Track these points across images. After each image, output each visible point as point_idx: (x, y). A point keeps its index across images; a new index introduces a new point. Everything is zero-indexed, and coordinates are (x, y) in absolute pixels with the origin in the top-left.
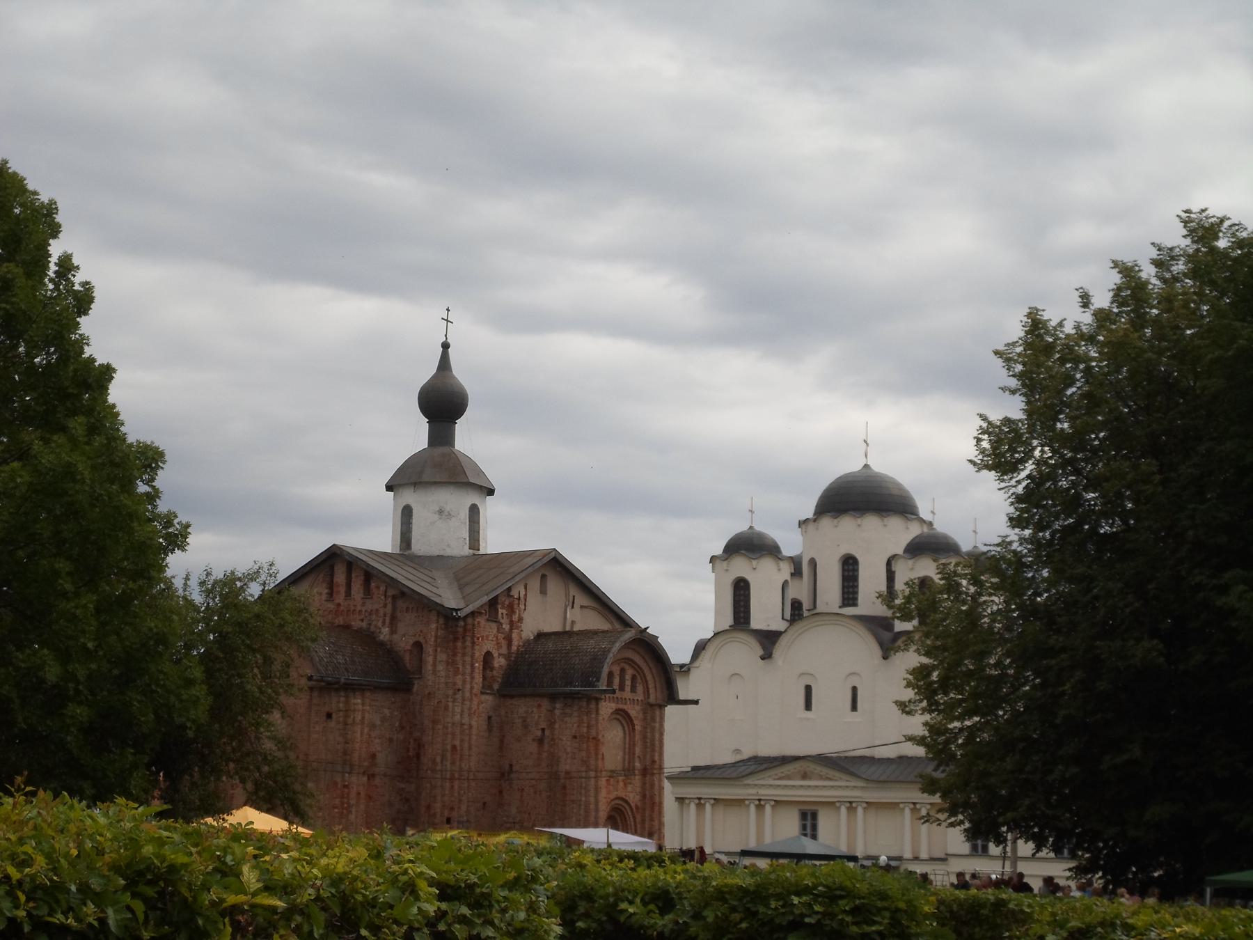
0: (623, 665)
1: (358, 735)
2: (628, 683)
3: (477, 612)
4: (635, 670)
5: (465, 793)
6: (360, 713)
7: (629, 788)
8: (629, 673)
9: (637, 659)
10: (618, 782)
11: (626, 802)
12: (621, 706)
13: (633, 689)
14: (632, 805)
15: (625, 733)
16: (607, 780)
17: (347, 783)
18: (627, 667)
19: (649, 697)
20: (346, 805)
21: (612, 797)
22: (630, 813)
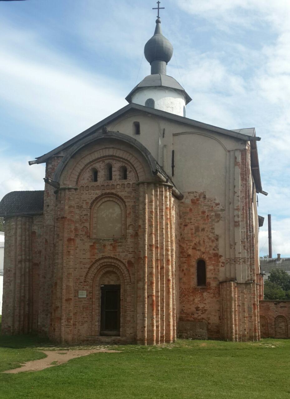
0: (107, 161)
1: (14, 242)
2: (116, 174)
3: (58, 157)
4: (123, 162)
5: (49, 267)
6: (14, 230)
7: (119, 249)
8: (116, 166)
9: (119, 153)
10: (104, 246)
11: (117, 259)
12: (108, 191)
13: (125, 177)
14: (124, 261)
15: (121, 210)
16: (90, 246)
17: (9, 269)
18: (113, 162)
19: (139, 180)
20: (9, 281)
21: (100, 256)
22: (123, 268)
